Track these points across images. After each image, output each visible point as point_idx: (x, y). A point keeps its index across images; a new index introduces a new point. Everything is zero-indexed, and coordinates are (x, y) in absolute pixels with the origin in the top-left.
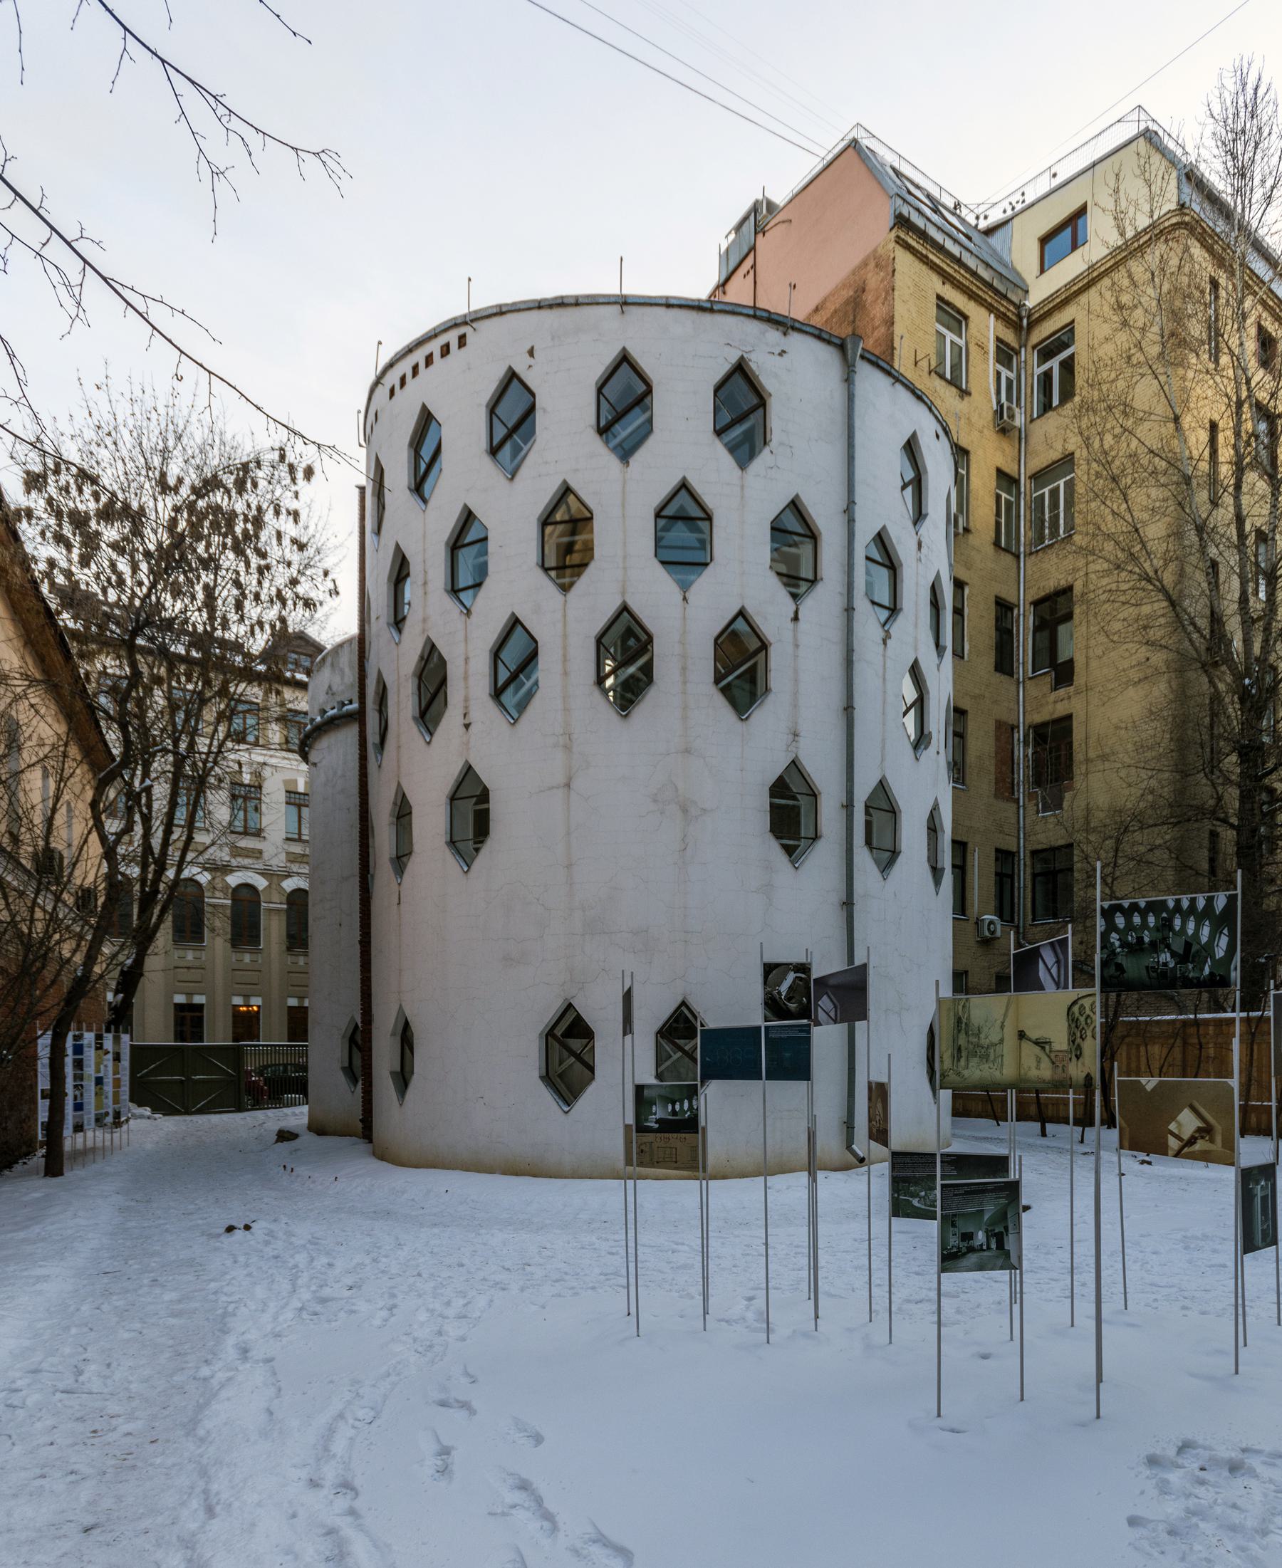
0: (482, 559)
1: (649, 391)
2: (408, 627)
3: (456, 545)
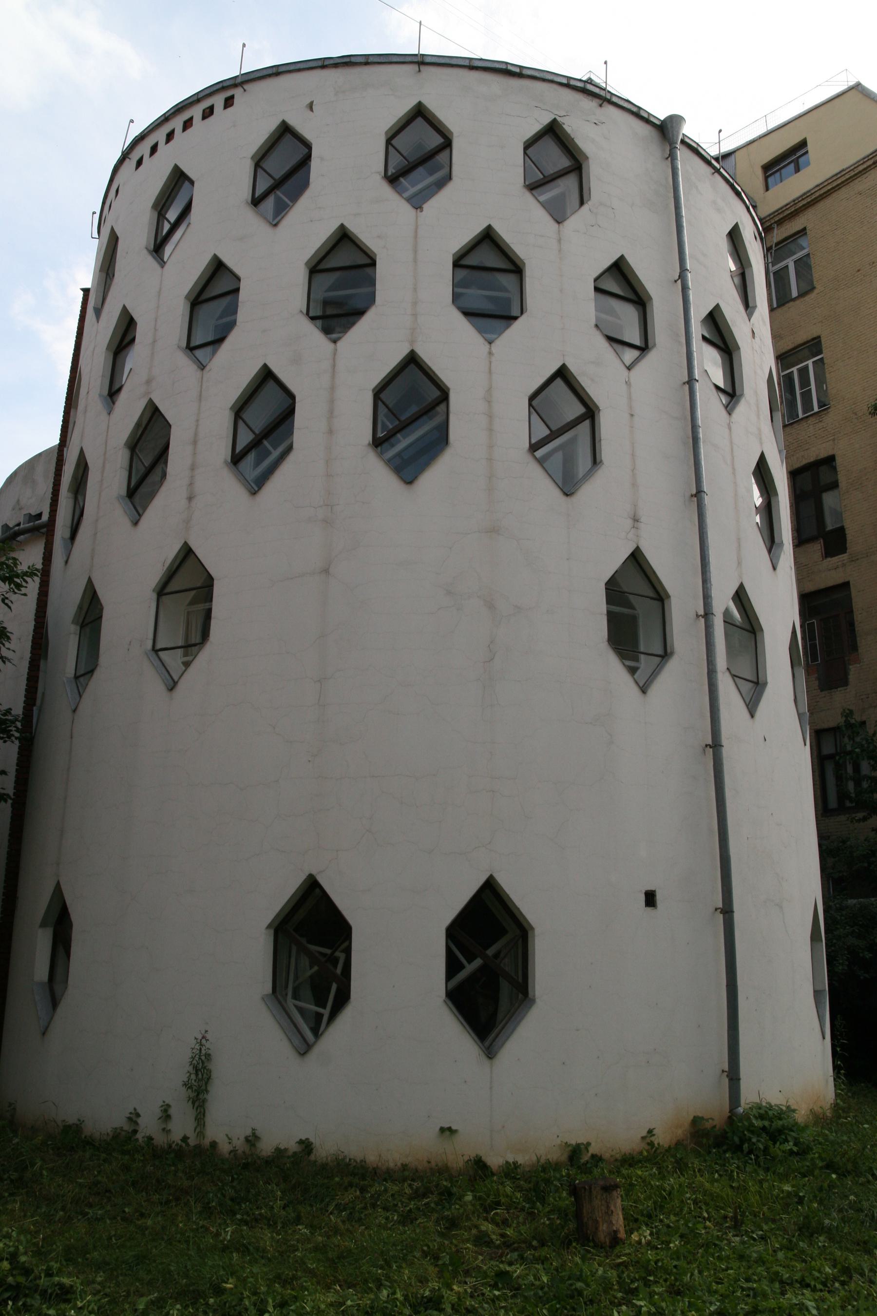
1: (447, 144)
3: (198, 300)
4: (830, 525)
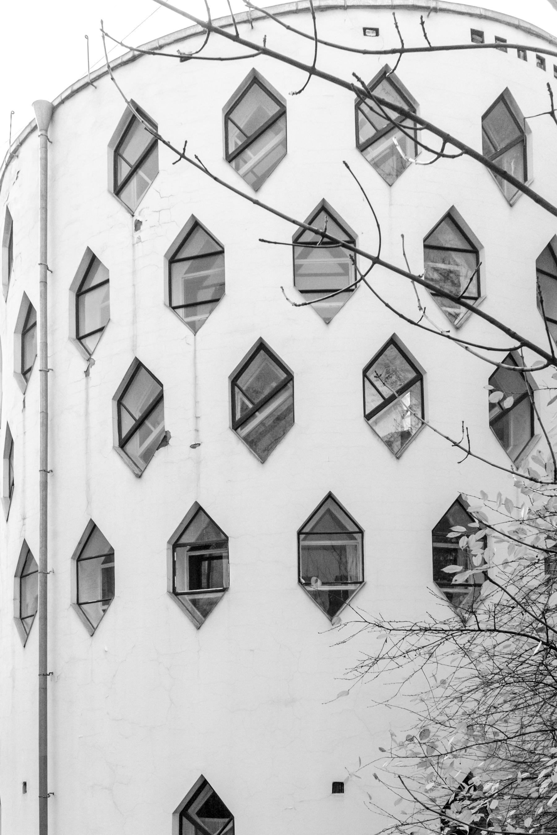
0: (106, 303)
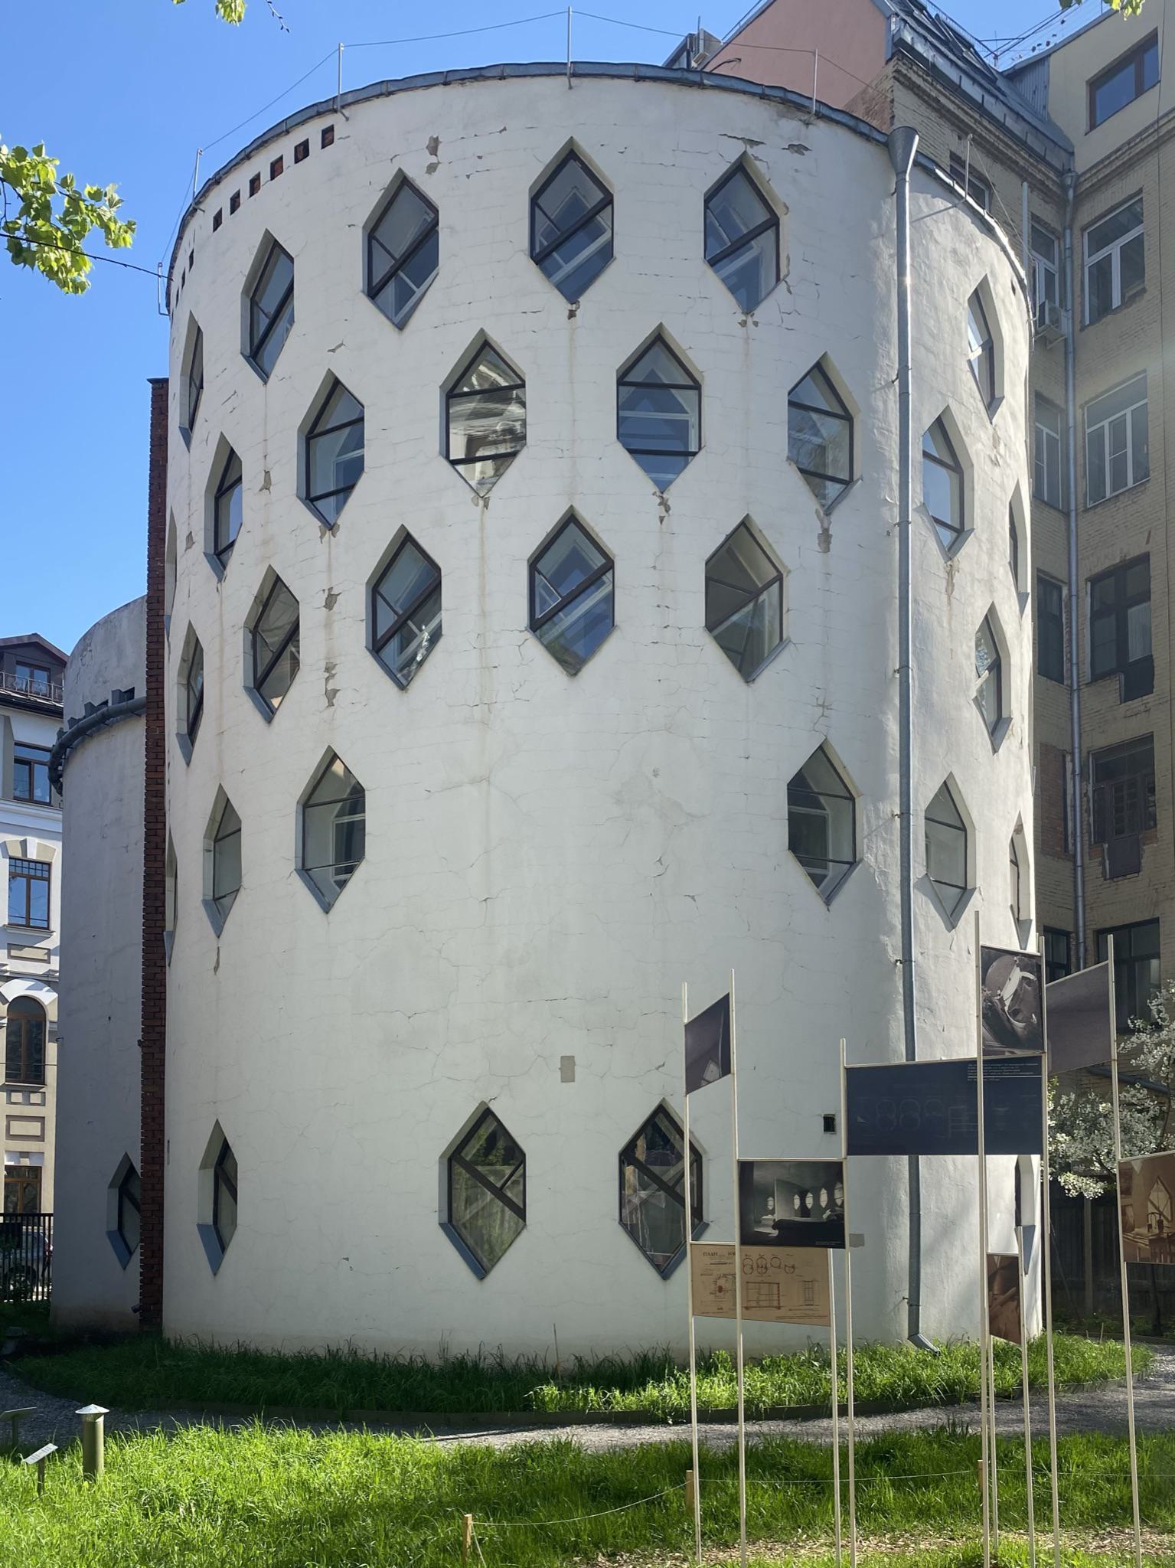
2: (236, 559)
3: (312, 433)
4: (1135, 653)
